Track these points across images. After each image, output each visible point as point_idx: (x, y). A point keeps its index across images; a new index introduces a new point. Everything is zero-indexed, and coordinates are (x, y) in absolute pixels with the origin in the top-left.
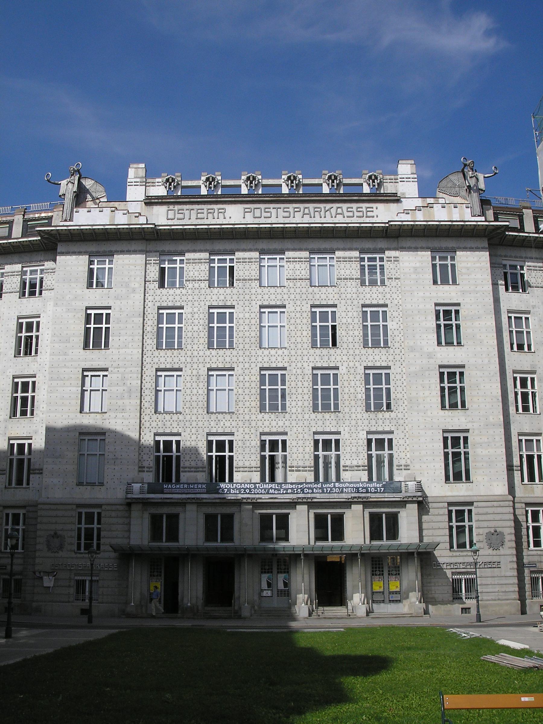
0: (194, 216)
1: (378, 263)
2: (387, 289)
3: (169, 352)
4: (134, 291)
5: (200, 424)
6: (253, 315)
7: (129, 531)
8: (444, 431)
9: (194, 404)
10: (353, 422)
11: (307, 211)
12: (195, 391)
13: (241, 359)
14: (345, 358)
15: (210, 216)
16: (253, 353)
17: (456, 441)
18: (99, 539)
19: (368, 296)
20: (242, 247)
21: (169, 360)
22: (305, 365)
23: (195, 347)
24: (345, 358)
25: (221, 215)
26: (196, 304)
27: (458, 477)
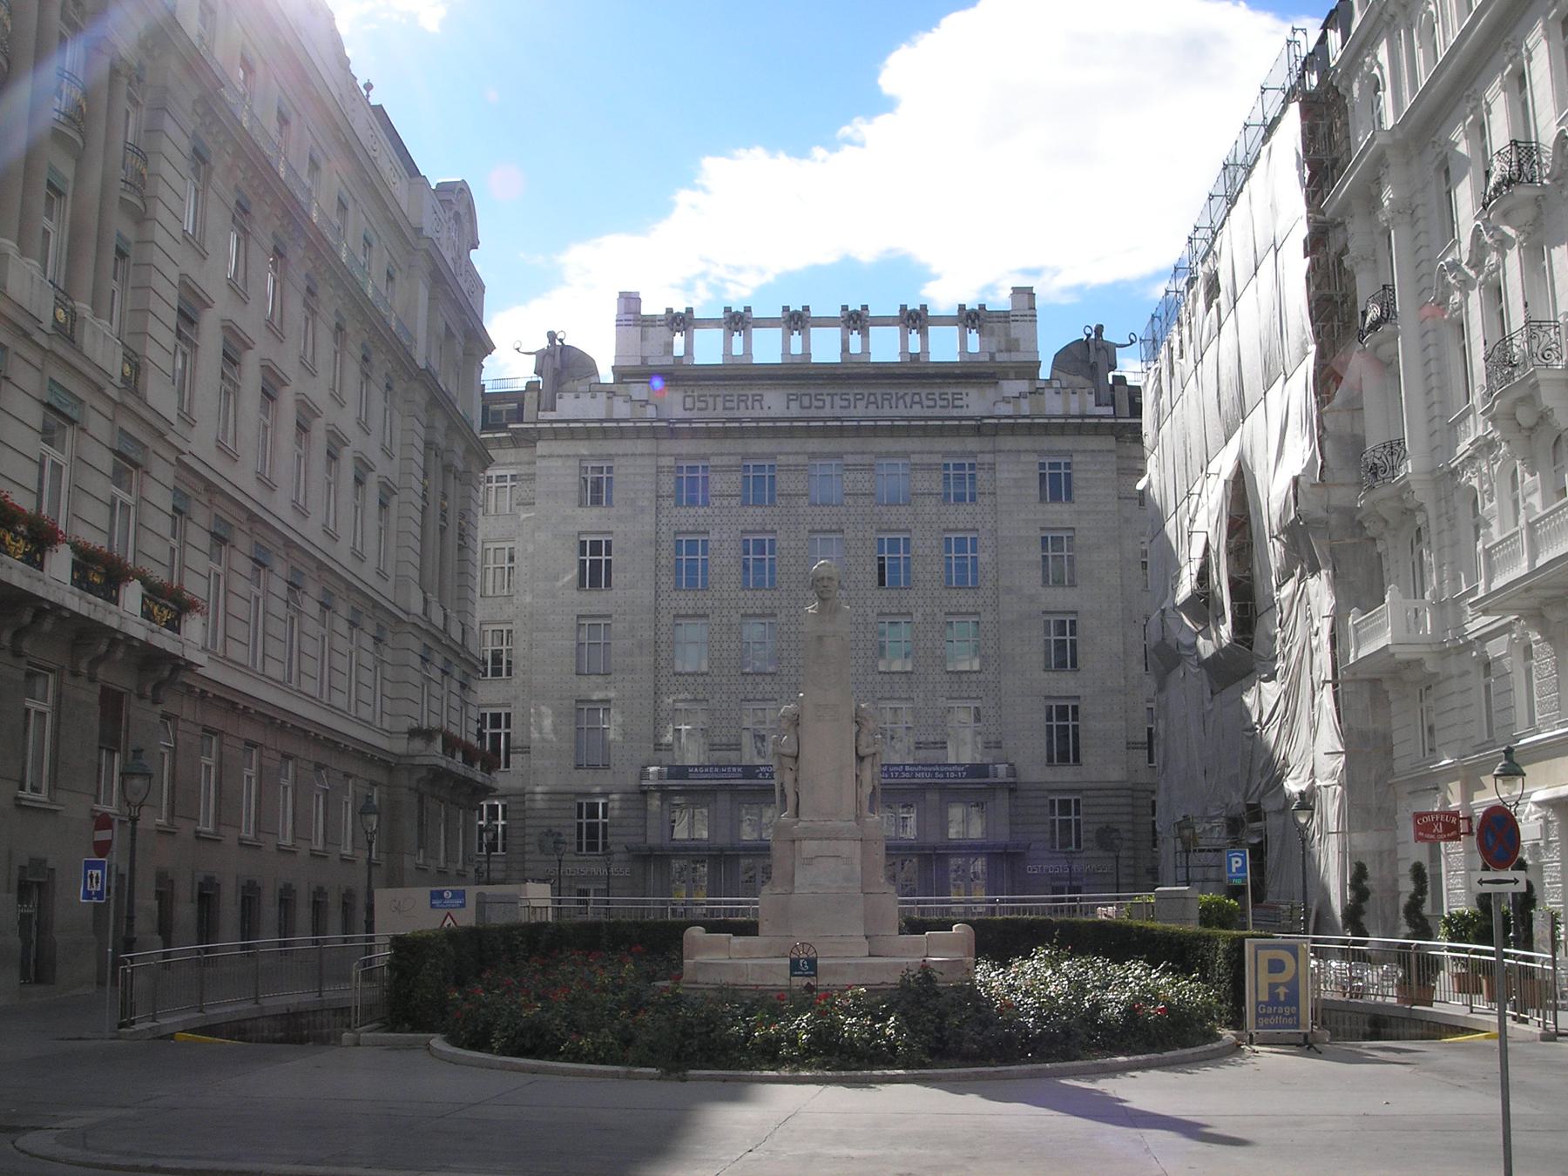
0: (720, 406)
1: (967, 472)
2: (978, 509)
3: (691, 595)
4: (642, 510)
5: (733, 688)
6: (800, 544)
7: (645, 826)
8: (1047, 698)
9: (725, 663)
10: (930, 687)
11: (872, 399)
12: (725, 646)
13: (785, 603)
14: (920, 602)
15: (742, 405)
16: (801, 595)
17: (1062, 712)
18: (605, 836)
19: (952, 518)
20: (788, 449)
21: (691, 604)
22: (869, 610)
23: (725, 587)
24: (920, 602)
25: (757, 405)
26: (725, 528)
27: (1064, 758)
